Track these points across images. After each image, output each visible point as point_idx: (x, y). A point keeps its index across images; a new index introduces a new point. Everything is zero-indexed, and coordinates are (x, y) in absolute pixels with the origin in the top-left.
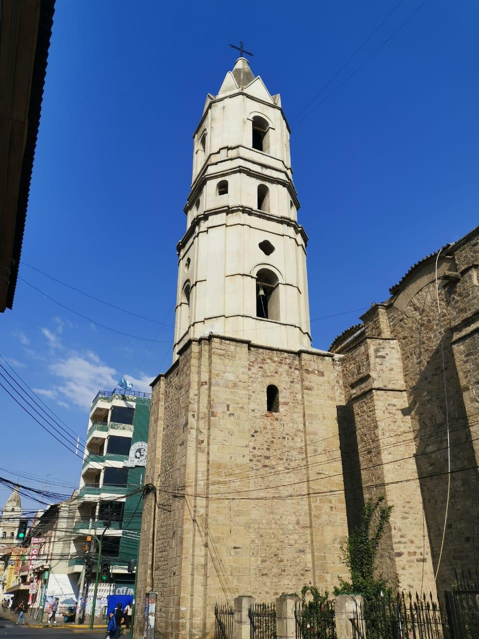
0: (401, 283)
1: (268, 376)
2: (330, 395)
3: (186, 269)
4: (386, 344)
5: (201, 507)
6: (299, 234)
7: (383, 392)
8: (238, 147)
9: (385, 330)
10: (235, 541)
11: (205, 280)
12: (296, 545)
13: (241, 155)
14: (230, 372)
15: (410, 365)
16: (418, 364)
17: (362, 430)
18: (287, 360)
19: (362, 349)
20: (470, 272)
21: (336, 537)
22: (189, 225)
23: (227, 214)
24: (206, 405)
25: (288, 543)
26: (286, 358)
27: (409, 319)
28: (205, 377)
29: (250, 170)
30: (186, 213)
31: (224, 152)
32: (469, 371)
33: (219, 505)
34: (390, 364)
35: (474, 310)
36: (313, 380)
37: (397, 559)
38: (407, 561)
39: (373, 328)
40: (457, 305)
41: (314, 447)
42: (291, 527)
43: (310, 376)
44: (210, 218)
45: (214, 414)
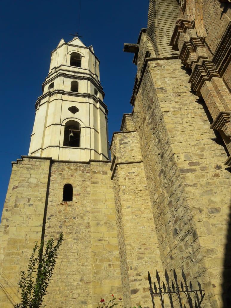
1: (66, 179)
4: (128, 135)
7: (125, 165)
12: (79, 298)
14: (33, 178)
18: (81, 168)
21: (113, 288)
25: (71, 297)
26: (80, 167)
28: (16, 183)
29: (65, 74)
33: (11, 271)
36: (99, 177)
37: (133, 296)
38: (142, 297)
41: (97, 221)
43: (97, 175)
45: (17, 206)
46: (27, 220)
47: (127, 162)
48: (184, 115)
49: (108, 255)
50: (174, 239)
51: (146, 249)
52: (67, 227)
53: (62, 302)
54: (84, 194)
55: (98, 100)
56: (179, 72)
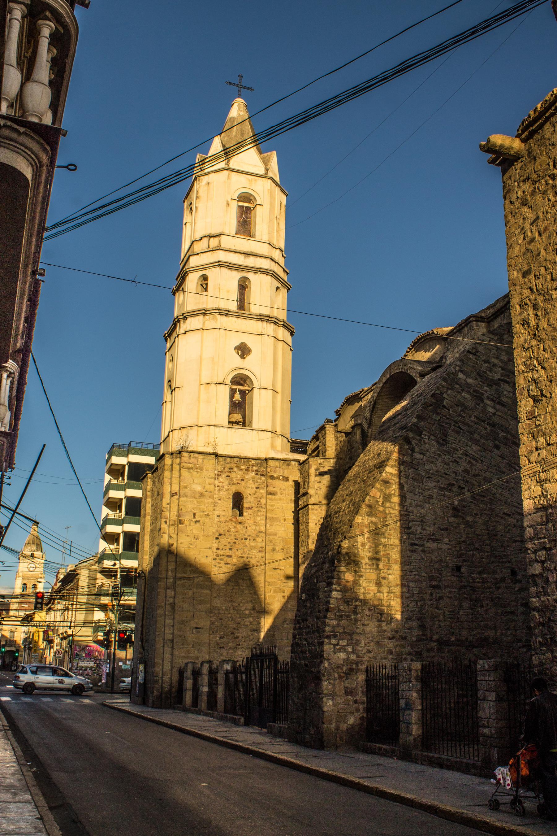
1: (233, 484)
5: (171, 597)
8: (219, 235)
10: (196, 623)
12: (251, 626)
13: (223, 246)
18: (254, 467)
24: (176, 513)
26: (253, 466)
28: (175, 488)
30: (174, 294)
31: (205, 240)
36: (278, 485)
42: (247, 612)
43: (276, 482)
44: (189, 319)
46: (195, 540)
53: (234, 629)
55: (282, 323)
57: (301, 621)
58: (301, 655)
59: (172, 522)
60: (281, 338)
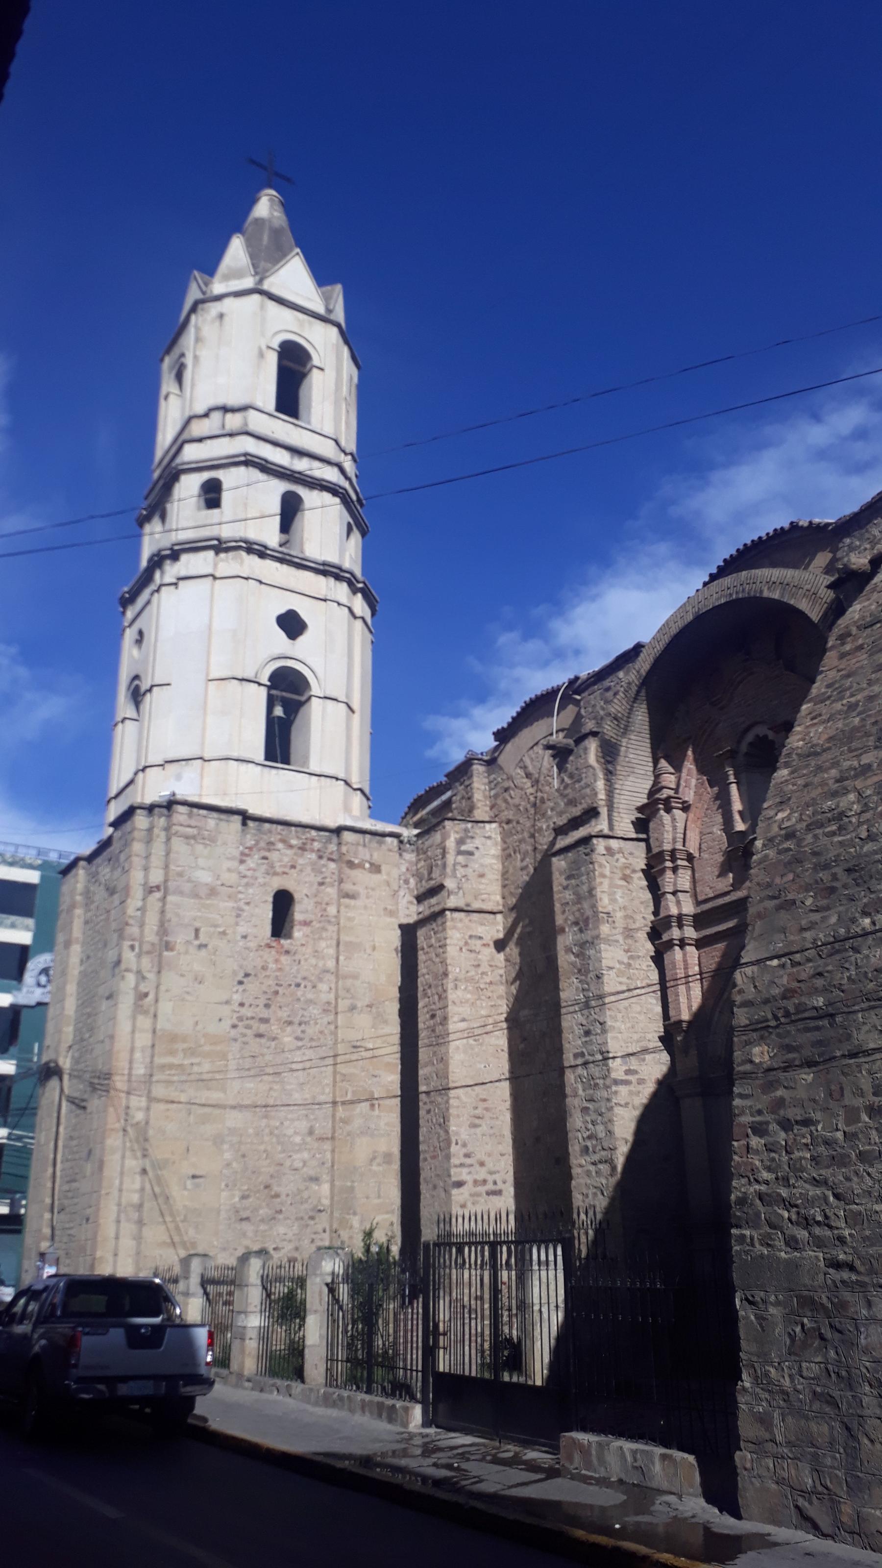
0: (510, 725)
1: (276, 874)
2: (389, 907)
3: (135, 652)
4: (477, 830)
5: (139, 1109)
6: (359, 595)
7: (462, 914)
9: (479, 805)
11: (168, 685)
12: (305, 1169)
13: (252, 427)
14: (203, 869)
15: (511, 870)
16: (522, 869)
17: (427, 977)
19: (437, 837)
20: (586, 742)
22: (144, 563)
23: (217, 554)
24: (155, 928)
25: (291, 1166)
26: (313, 840)
27: (517, 790)
28: (156, 877)
29: (266, 461)
31: (216, 416)
32: (568, 903)
34: (481, 865)
35: (585, 806)
36: (361, 879)
37: (454, 1191)
38: (471, 1195)
39: (463, 798)
40: (566, 792)
41: (351, 1001)
42: (298, 1139)
43: (357, 874)
44: (184, 557)
47: (469, 909)
48: (632, 979)
49: (370, 1082)
50: (581, 1155)
51: (487, 1109)
52: (280, 1007)
54: (320, 922)
55: (360, 585)
56: (640, 879)
57: (773, 1127)
58: (802, 1234)
59: (146, 947)
60: (358, 611)
